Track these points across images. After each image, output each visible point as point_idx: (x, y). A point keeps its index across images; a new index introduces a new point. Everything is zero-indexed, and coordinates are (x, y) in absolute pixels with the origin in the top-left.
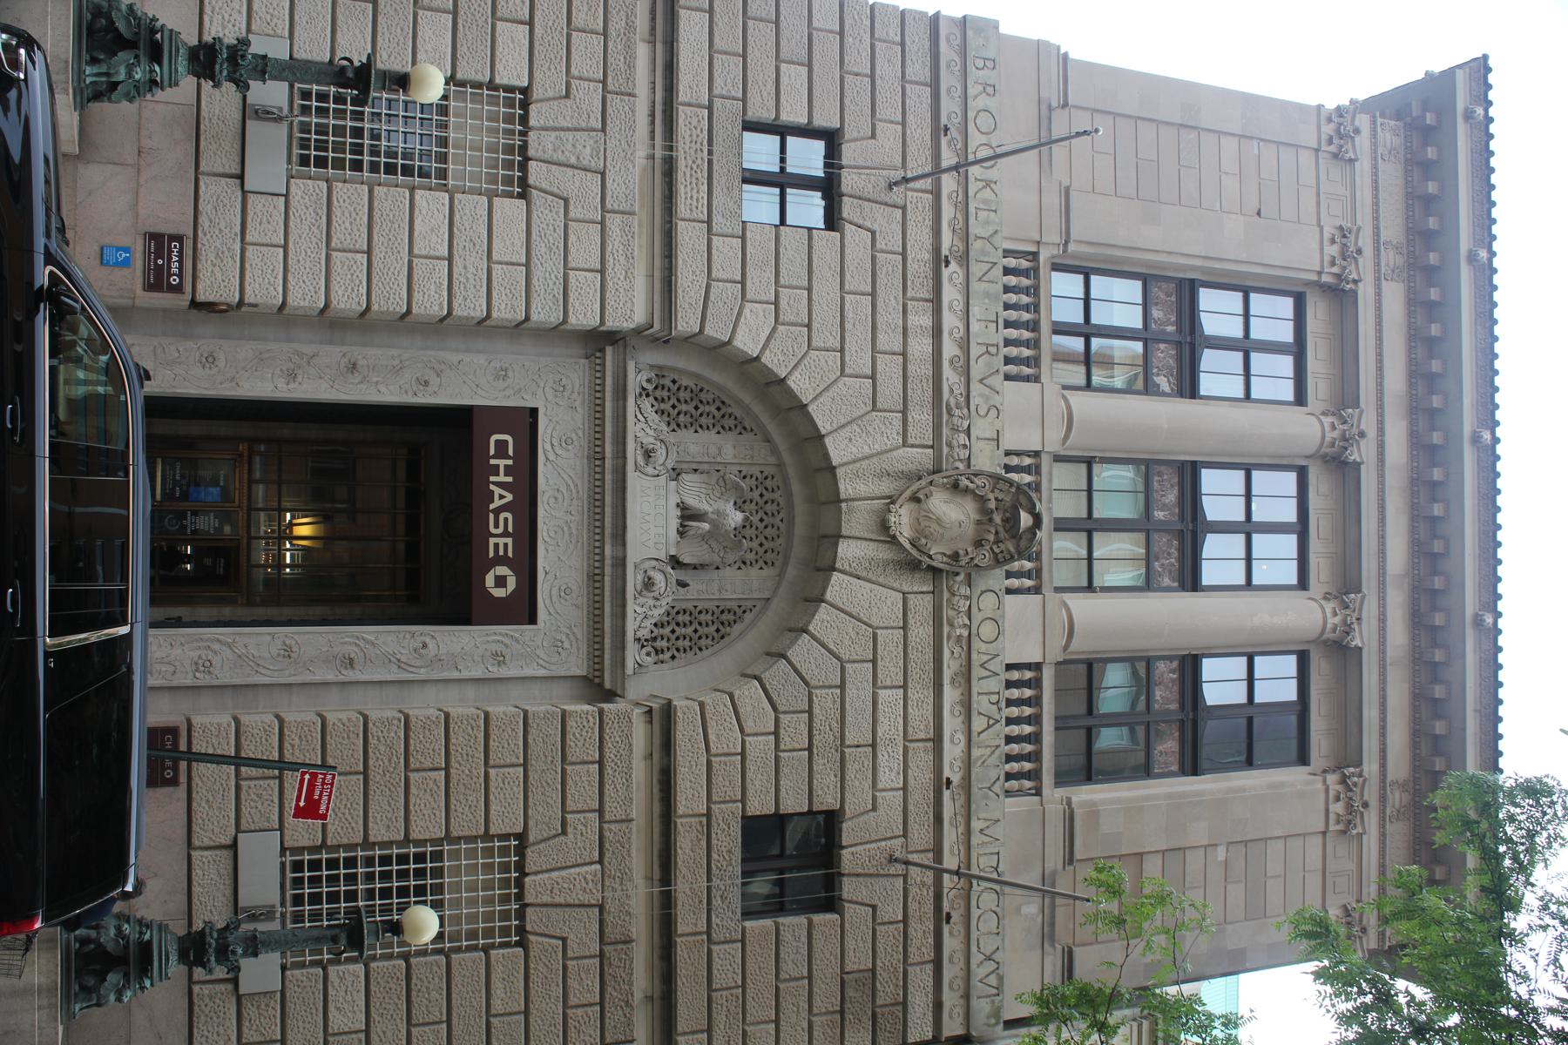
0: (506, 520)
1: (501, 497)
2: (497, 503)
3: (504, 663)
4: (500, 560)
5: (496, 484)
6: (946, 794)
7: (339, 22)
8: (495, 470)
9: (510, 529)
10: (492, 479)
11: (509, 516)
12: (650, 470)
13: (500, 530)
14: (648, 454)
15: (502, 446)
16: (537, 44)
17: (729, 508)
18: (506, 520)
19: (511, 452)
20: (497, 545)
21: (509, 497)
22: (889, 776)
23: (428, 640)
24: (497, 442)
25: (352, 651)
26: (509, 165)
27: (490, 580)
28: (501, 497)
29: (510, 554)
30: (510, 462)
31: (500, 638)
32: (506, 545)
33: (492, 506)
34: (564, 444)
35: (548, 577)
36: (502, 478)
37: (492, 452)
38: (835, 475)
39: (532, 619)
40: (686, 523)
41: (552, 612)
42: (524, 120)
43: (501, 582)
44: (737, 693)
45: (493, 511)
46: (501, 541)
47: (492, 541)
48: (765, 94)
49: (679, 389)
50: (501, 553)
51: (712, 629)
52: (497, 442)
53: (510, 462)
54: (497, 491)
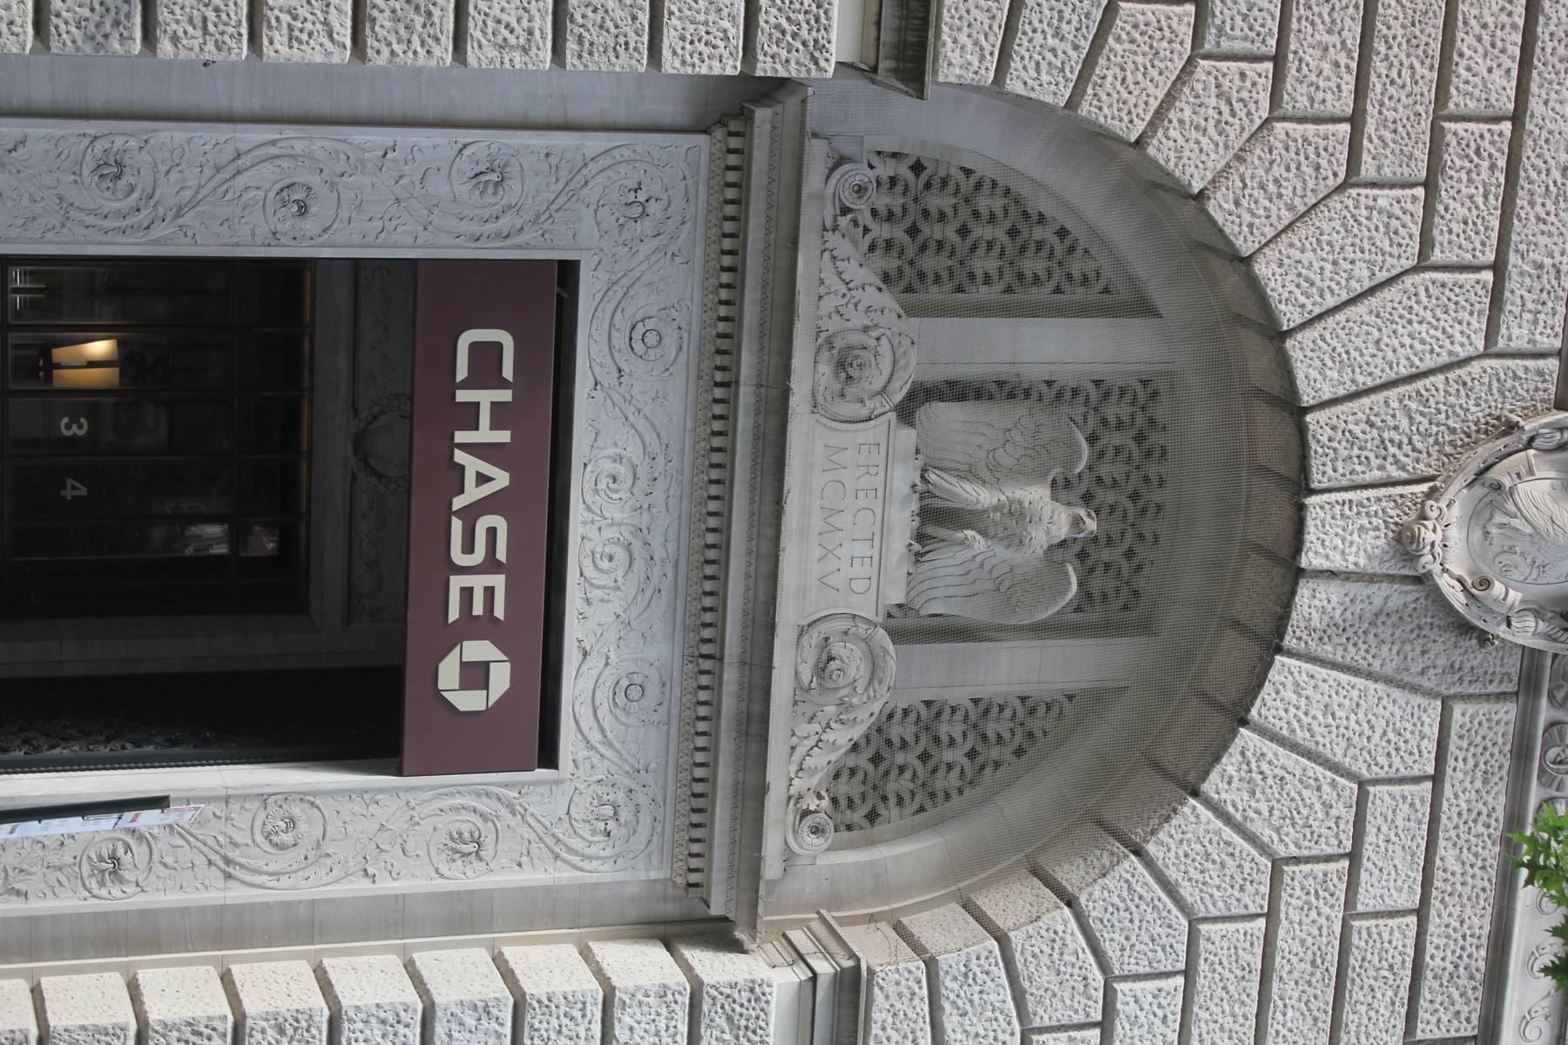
0: (492, 532)
1: (482, 479)
2: (472, 494)
3: (480, 859)
4: (473, 627)
5: (468, 448)
8: (469, 419)
9: (501, 555)
10: (461, 437)
11: (500, 523)
12: (848, 409)
13: (478, 557)
14: (846, 366)
15: (487, 357)
17: (1037, 495)
18: (492, 532)
19: (508, 372)
20: (467, 593)
21: (501, 479)
23: (295, 809)
24: (475, 347)
27: (448, 673)
28: (482, 479)
29: (499, 613)
30: (505, 396)
31: (471, 802)
32: (490, 592)
33: (458, 503)
34: (638, 346)
35: (590, 662)
36: (485, 434)
37: (462, 373)
38: (1302, 430)
39: (548, 756)
40: (931, 530)
41: (595, 737)
43: (476, 675)
44: (1017, 938)
45: (459, 513)
46: (478, 583)
47: (457, 583)
49: (928, 185)
50: (478, 609)
52: (475, 347)
53: (505, 396)
54: (472, 465)
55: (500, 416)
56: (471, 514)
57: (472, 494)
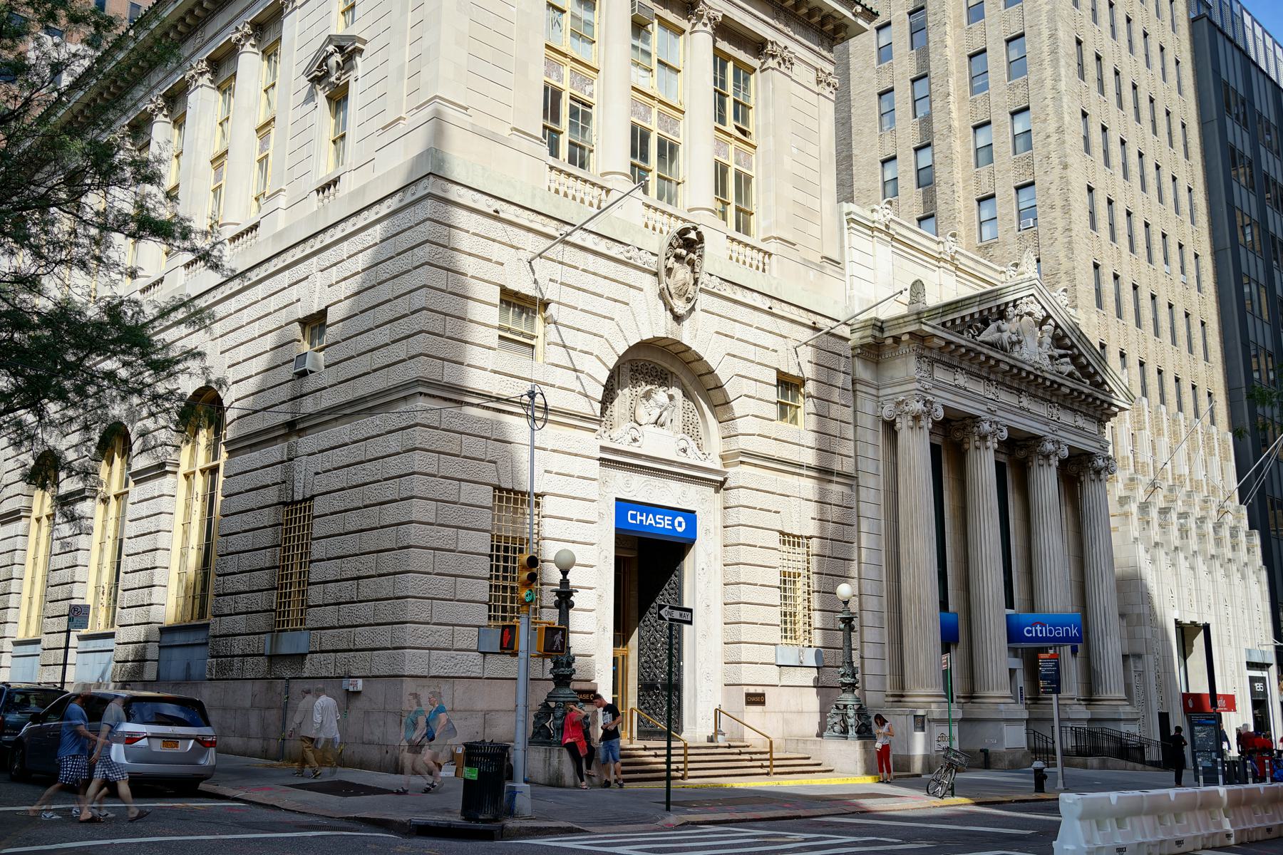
2: (653, 522)
4: (673, 525)
6: (774, 311)
7: (469, 598)
14: (635, 440)
16: (472, 479)
21: (651, 516)
22: (769, 340)
25: (704, 605)
26: (508, 500)
36: (644, 518)
39: (694, 512)
42: (509, 491)
48: (487, 334)
51: (691, 415)
54: (649, 522)
55: (641, 515)
56: (656, 523)
57: (653, 522)
